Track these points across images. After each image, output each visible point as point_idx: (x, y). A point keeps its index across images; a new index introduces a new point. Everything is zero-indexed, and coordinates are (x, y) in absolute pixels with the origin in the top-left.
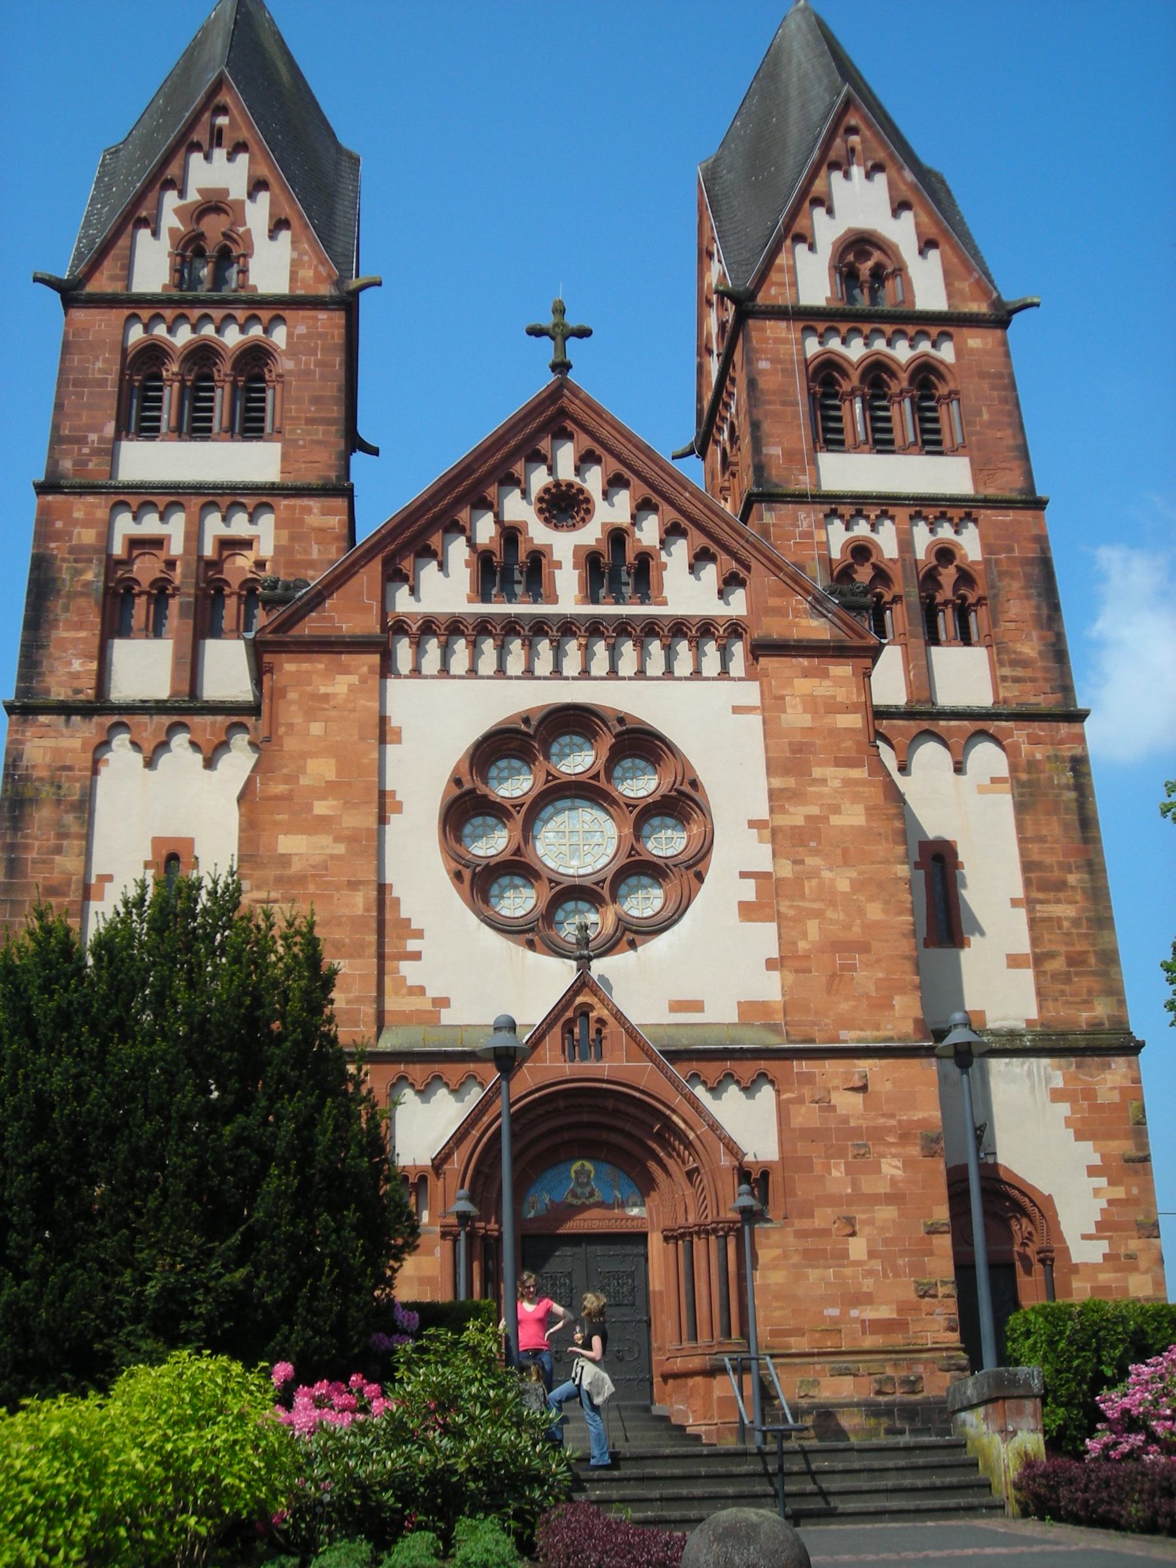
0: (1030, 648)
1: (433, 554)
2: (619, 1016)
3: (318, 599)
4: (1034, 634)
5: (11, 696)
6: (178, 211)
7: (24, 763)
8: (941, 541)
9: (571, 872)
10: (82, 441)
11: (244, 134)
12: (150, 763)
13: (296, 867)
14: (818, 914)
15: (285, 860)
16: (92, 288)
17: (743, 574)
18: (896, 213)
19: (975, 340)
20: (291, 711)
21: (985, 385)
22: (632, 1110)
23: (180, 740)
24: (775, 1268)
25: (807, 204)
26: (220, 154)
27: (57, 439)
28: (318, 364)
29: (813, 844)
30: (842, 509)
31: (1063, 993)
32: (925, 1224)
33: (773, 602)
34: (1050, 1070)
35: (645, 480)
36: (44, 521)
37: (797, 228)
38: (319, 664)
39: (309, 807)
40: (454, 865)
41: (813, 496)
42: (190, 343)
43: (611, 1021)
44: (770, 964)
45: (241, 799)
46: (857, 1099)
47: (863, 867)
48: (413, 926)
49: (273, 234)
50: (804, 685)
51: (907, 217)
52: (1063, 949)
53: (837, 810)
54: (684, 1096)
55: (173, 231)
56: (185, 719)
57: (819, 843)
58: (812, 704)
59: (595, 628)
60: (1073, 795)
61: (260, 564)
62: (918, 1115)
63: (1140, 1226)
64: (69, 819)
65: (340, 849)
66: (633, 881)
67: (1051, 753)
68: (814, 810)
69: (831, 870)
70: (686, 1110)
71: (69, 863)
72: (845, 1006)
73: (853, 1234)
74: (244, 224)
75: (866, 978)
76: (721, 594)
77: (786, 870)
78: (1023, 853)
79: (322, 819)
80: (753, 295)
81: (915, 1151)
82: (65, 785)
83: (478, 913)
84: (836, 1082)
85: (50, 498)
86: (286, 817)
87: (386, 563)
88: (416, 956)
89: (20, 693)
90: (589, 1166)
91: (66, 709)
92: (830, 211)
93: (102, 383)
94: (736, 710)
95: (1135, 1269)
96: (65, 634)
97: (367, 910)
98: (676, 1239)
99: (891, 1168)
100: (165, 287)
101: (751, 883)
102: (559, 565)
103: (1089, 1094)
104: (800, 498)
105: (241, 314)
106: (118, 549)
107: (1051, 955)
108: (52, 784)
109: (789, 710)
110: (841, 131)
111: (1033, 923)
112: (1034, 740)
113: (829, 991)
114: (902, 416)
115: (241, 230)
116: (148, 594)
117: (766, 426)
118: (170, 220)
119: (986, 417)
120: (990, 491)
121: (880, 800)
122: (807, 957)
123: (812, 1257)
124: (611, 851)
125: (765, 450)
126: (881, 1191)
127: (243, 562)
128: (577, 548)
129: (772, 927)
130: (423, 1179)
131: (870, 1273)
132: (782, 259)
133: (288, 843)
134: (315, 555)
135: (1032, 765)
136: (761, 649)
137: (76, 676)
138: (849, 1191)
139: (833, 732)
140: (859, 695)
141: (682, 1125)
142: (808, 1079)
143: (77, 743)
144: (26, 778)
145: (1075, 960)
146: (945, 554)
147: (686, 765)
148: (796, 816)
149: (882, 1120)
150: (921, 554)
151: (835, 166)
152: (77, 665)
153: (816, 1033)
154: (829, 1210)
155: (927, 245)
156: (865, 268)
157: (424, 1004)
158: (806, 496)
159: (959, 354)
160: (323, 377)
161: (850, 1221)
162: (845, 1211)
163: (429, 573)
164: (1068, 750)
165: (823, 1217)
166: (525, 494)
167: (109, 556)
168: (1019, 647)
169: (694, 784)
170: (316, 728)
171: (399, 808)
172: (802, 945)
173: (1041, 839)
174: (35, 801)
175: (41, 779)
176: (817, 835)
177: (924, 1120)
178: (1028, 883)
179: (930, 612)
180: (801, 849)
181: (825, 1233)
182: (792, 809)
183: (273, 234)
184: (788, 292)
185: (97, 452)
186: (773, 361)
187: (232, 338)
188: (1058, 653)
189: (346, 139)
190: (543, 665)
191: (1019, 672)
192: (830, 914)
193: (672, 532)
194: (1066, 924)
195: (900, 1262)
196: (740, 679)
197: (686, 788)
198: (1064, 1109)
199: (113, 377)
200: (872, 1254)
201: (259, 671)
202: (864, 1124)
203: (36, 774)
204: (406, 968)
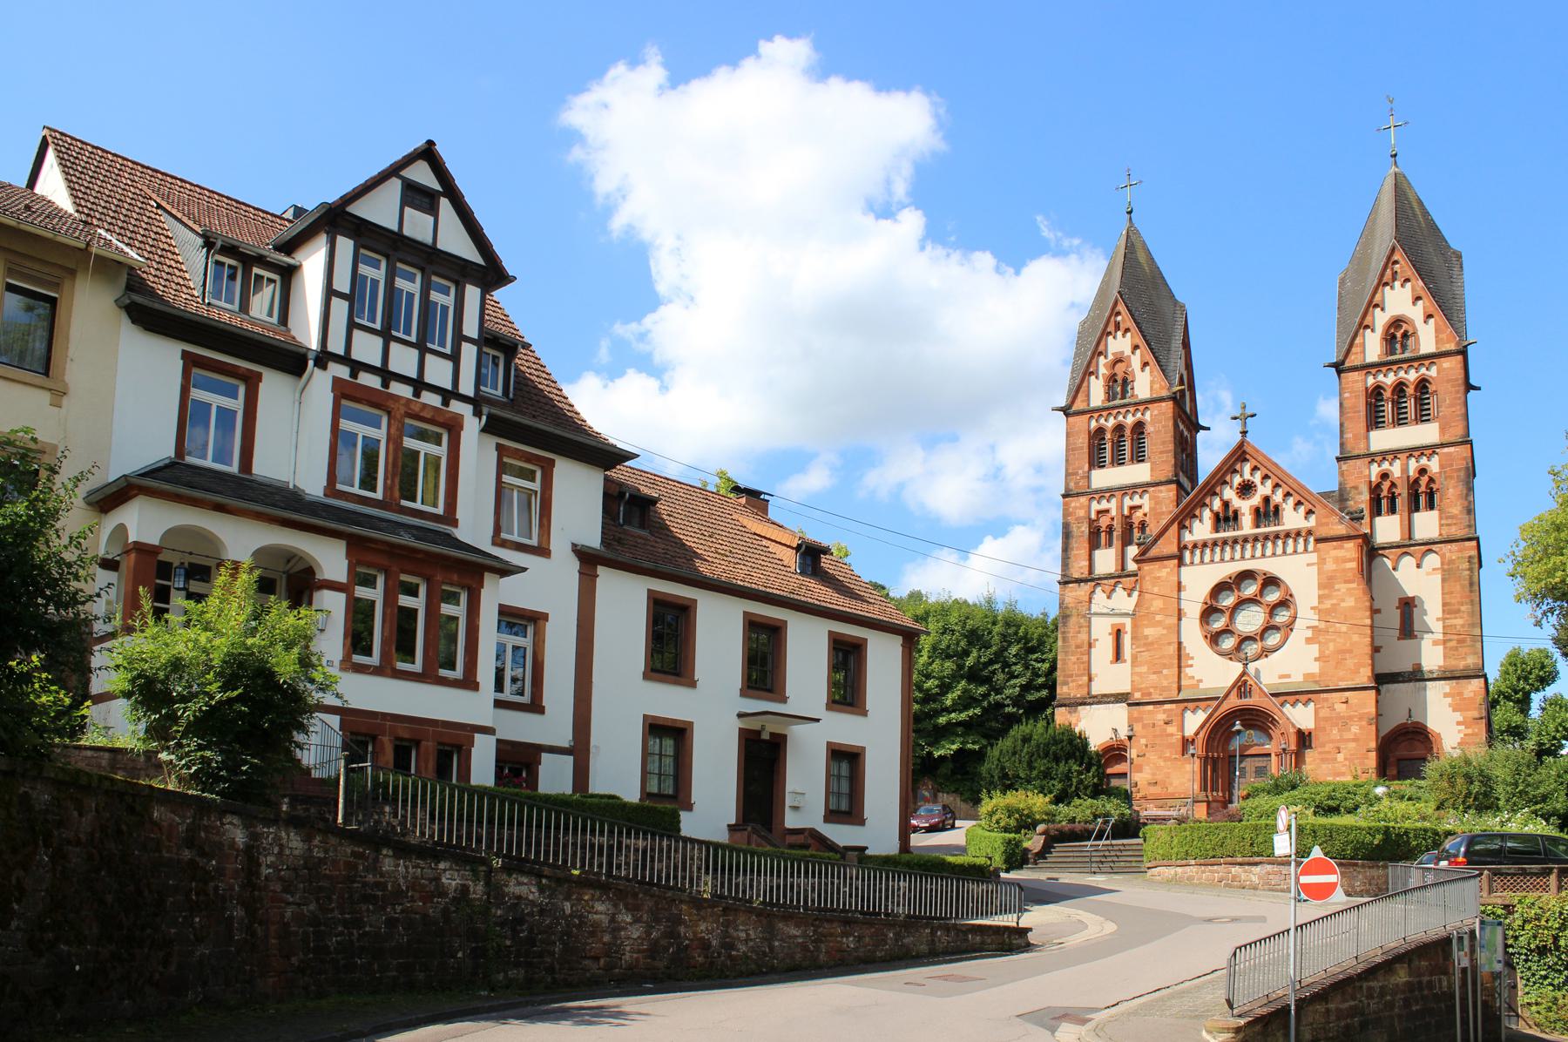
0: (1456, 509)
1: (1195, 516)
5: (1059, 578)
10: (1076, 474)
12: (1109, 597)
14: (1334, 640)
15: (1146, 637)
16: (1075, 408)
17: (1314, 509)
18: (1414, 303)
19: (1448, 363)
21: (1449, 386)
23: (1119, 589)
26: (1119, 334)
27: (1067, 475)
28: (1163, 427)
30: (1376, 459)
36: (1065, 504)
38: (1156, 565)
44: (1316, 659)
49: (1143, 370)
53: (1343, 600)
61: (1145, 515)
62: (1366, 711)
65: (1165, 632)
66: (1270, 632)
68: (1334, 601)
71: (1083, 637)
72: (1342, 673)
75: (1350, 663)
77: (1322, 625)
80: (1343, 363)
81: (1364, 723)
83: (1212, 648)
87: (1179, 524)
88: (1191, 666)
91: (1079, 581)
92: (1383, 309)
93: (1082, 448)
94: (1308, 565)
99: (1355, 729)
100: (1103, 401)
102: (1244, 514)
104: (1358, 457)
105: (1132, 409)
117: (1346, 424)
118: (1103, 370)
119: (1448, 402)
120: (1447, 438)
121: (1361, 595)
125: (1345, 436)
127: (1138, 515)
129: (1317, 646)
130: (1193, 740)
132: (1358, 341)
133: (1148, 631)
134: (1164, 509)
137: (1081, 568)
139: (1344, 570)
142: (1326, 700)
143: (1083, 593)
144: (1067, 608)
146: (1423, 471)
147: (1287, 587)
148: (1328, 604)
150: (1411, 473)
156: (1399, 335)
161: (1339, 748)
162: (1337, 745)
163: (1196, 524)
167: (1090, 519)
169: (1291, 595)
172: (1327, 652)
181: (1329, 752)
183: (1143, 370)
184: (1360, 357)
185: (1082, 478)
187: (1130, 420)
188: (1470, 511)
189: (1180, 296)
190: (1238, 555)
191: (1449, 521)
192: (1338, 640)
197: (1288, 597)
199: (1086, 445)
203: (1070, 606)
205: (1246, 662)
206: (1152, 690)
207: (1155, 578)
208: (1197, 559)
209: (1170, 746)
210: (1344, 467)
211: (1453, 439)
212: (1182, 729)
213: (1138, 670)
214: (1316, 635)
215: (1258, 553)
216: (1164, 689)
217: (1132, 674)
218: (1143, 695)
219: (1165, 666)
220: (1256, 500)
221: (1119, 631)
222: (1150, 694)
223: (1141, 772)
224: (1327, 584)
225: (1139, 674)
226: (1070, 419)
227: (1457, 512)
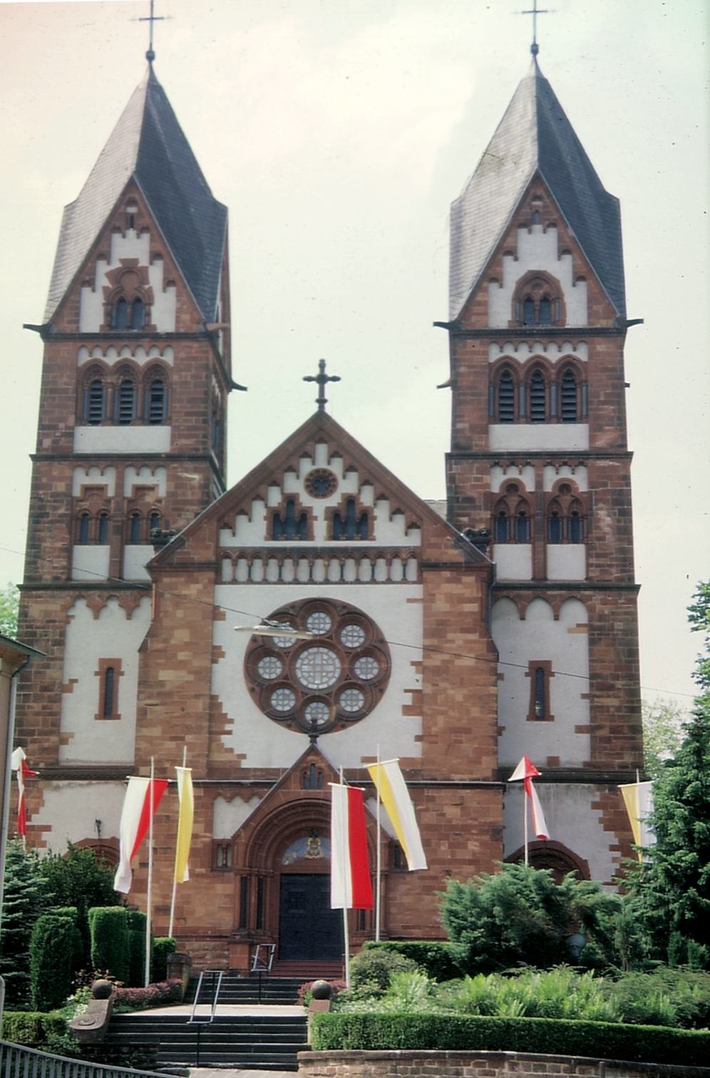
6: (109, 275)
9: (315, 687)
11: (145, 221)
13: (168, 688)
14: (444, 713)
15: (162, 684)
19: (602, 346)
24: (407, 894)
33: (433, 540)
39: (175, 656)
40: (251, 685)
42: (118, 363)
44: (418, 738)
47: (471, 688)
48: (229, 717)
51: (568, 259)
53: (459, 656)
55: (105, 289)
58: (451, 598)
65: (191, 678)
68: (446, 657)
69: (453, 689)
74: (148, 283)
77: (429, 690)
79: (181, 662)
81: (486, 838)
84: (446, 802)
86: (163, 661)
88: (229, 733)
93: (66, 391)
94: (409, 601)
97: (204, 709)
99: (473, 846)
100: (101, 326)
101: (411, 694)
102: (316, 518)
109: (437, 602)
110: (528, 200)
114: (552, 396)
115: (147, 287)
118: (103, 281)
122: (436, 736)
126: (467, 858)
133: (166, 675)
138: (449, 857)
139: (461, 614)
140: (478, 593)
142: (432, 799)
148: (437, 660)
149: (470, 822)
153: (437, 775)
154: (438, 866)
155: (578, 278)
156: (538, 294)
159: (591, 355)
162: (446, 867)
170: (180, 613)
171: (222, 655)
177: (493, 822)
180: (437, 678)
182: (434, 656)
186: (469, 367)
187: (142, 359)
190: (304, 576)
192: (451, 713)
193: (380, 497)
196: (414, 583)
197: (378, 645)
202: (460, 823)
204: (224, 738)
205: (314, 731)
207: (178, 596)
213: (145, 732)
214: (418, 705)
215: (335, 576)
217: (138, 738)
220: (334, 500)
221: (110, 670)
224: (435, 630)
225: (150, 740)
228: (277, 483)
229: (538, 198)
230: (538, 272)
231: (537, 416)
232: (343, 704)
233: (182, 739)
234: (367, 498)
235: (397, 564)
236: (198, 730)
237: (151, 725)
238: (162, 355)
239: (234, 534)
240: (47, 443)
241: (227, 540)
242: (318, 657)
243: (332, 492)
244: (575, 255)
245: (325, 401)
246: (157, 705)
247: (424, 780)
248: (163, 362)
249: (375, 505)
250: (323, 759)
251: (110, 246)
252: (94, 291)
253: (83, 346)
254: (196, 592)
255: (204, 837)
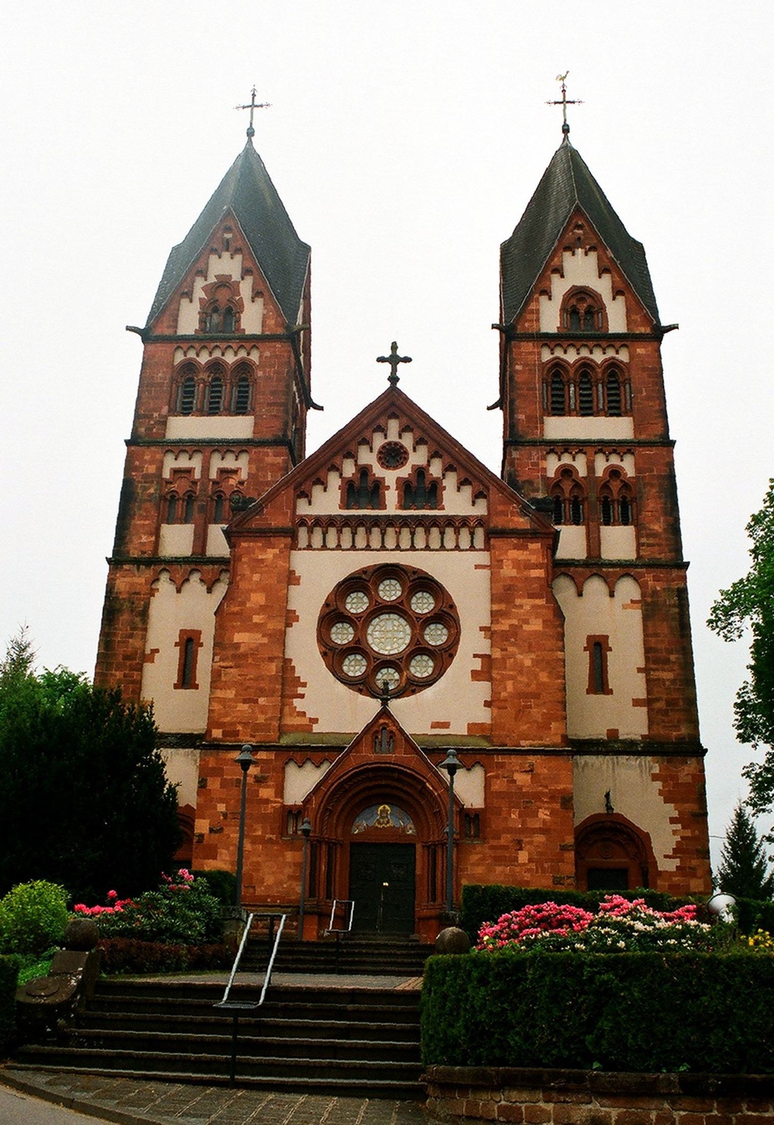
2: (401, 731)
3: (259, 509)
4: (662, 519)
7: (116, 590)
8: (612, 466)
9: (386, 653)
11: (239, 244)
12: (179, 591)
15: (237, 646)
20: (244, 568)
22: (407, 779)
23: (195, 578)
24: (478, 865)
25: (549, 272)
29: (513, 640)
31: (663, 721)
32: (560, 845)
33: (500, 508)
34: (652, 763)
35: (435, 441)
37: (541, 286)
39: (251, 619)
41: (540, 442)
43: (397, 733)
44: (487, 704)
45: (215, 614)
46: (528, 777)
48: (302, 681)
50: (514, 554)
51: (607, 278)
52: (665, 697)
53: (527, 622)
54: (433, 773)
56: (198, 567)
57: (516, 640)
58: (517, 564)
59: (404, 522)
60: (677, 610)
63: (698, 851)
64: (138, 619)
67: (666, 586)
68: (515, 622)
70: (434, 780)
71: (135, 643)
73: (521, 849)
76: (474, 503)
77: (497, 654)
78: (645, 642)
81: (557, 806)
82: (136, 602)
83: (334, 674)
84: (518, 768)
85: (133, 448)
88: (302, 696)
89: (115, 552)
90: (387, 807)
91: (137, 562)
93: (161, 385)
94: (477, 567)
95: (694, 876)
96: (138, 522)
98: (429, 847)
99: (544, 814)
101: (479, 660)
102: (388, 488)
103: (674, 778)
104: (534, 443)
106: (166, 475)
107: (657, 700)
108: (129, 601)
110: (571, 228)
111: (648, 681)
112: (656, 579)
113: (516, 719)
115: (237, 298)
116: (183, 500)
119: (644, 394)
120: (643, 437)
123: (498, 860)
124: (407, 641)
128: (398, 479)
131: (529, 870)
132: (532, 306)
133: (238, 637)
135: (655, 593)
136: (492, 534)
137: (144, 544)
139: (527, 579)
141: (431, 788)
142: (501, 766)
143: (143, 580)
145: (670, 703)
146: (615, 472)
148: (504, 625)
151: (567, 249)
152: (144, 539)
155: (617, 292)
156: (582, 308)
157: (304, 721)
158: (536, 442)
160: (278, 380)
161: (519, 842)
162: (518, 837)
164: (675, 585)
165: (506, 839)
166: (371, 451)
168: (652, 527)
170: (256, 577)
171: (297, 619)
173: (656, 635)
174: (120, 611)
175: (124, 599)
176: (515, 635)
177: (564, 789)
178: (647, 659)
179: (606, 505)
186: (525, 365)
187: (230, 358)
190: (376, 544)
191: (651, 541)
193: (448, 468)
194: (667, 683)
195: (546, 865)
196: (480, 550)
198: (658, 785)
200: (530, 860)
201: (232, 545)
204: (296, 702)
205: (385, 695)
206: (240, 728)
208: (317, 541)
209: (264, 818)
210: (515, 455)
211: (653, 439)
212: (280, 792)
213: (219, 694)
215: (405, 544)
216: (257, 728)
218: (224, 733)
219: (262, 692)
222: (237, 733)
223: (215, 858)
225: (222, 701)
226: (151, 347)
227: (660, 530)
228: (352, 455)
229: (579, 227)
230: (581, 287)
231: (586, 410)
232: (412, 670)
233: (257, 701)
234: (436, 470)
235: (465, 533)
236: (270, 694)
237: (226, 686)
238: (249, 354)
239: (310, 503)
240: (142, 430)
241: (303, 509)
242: (389, 622)
243: (403, 464)
244: (613, 273)
245: (398, 379)
246: (231, 667)
247: (494, 746)
248: (251, 360)
249: (444, 475)
250: (395, 722)
251: (207, 264)
252: (191, 301)
253: (179, 347)
254: (271, 556)
255: (275, 802)
